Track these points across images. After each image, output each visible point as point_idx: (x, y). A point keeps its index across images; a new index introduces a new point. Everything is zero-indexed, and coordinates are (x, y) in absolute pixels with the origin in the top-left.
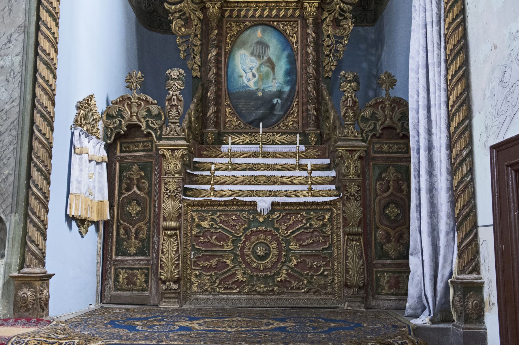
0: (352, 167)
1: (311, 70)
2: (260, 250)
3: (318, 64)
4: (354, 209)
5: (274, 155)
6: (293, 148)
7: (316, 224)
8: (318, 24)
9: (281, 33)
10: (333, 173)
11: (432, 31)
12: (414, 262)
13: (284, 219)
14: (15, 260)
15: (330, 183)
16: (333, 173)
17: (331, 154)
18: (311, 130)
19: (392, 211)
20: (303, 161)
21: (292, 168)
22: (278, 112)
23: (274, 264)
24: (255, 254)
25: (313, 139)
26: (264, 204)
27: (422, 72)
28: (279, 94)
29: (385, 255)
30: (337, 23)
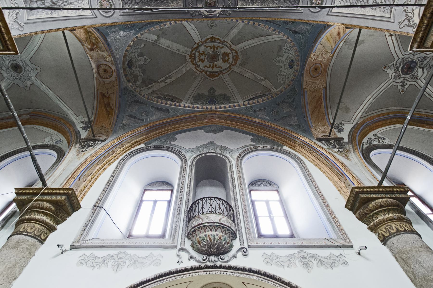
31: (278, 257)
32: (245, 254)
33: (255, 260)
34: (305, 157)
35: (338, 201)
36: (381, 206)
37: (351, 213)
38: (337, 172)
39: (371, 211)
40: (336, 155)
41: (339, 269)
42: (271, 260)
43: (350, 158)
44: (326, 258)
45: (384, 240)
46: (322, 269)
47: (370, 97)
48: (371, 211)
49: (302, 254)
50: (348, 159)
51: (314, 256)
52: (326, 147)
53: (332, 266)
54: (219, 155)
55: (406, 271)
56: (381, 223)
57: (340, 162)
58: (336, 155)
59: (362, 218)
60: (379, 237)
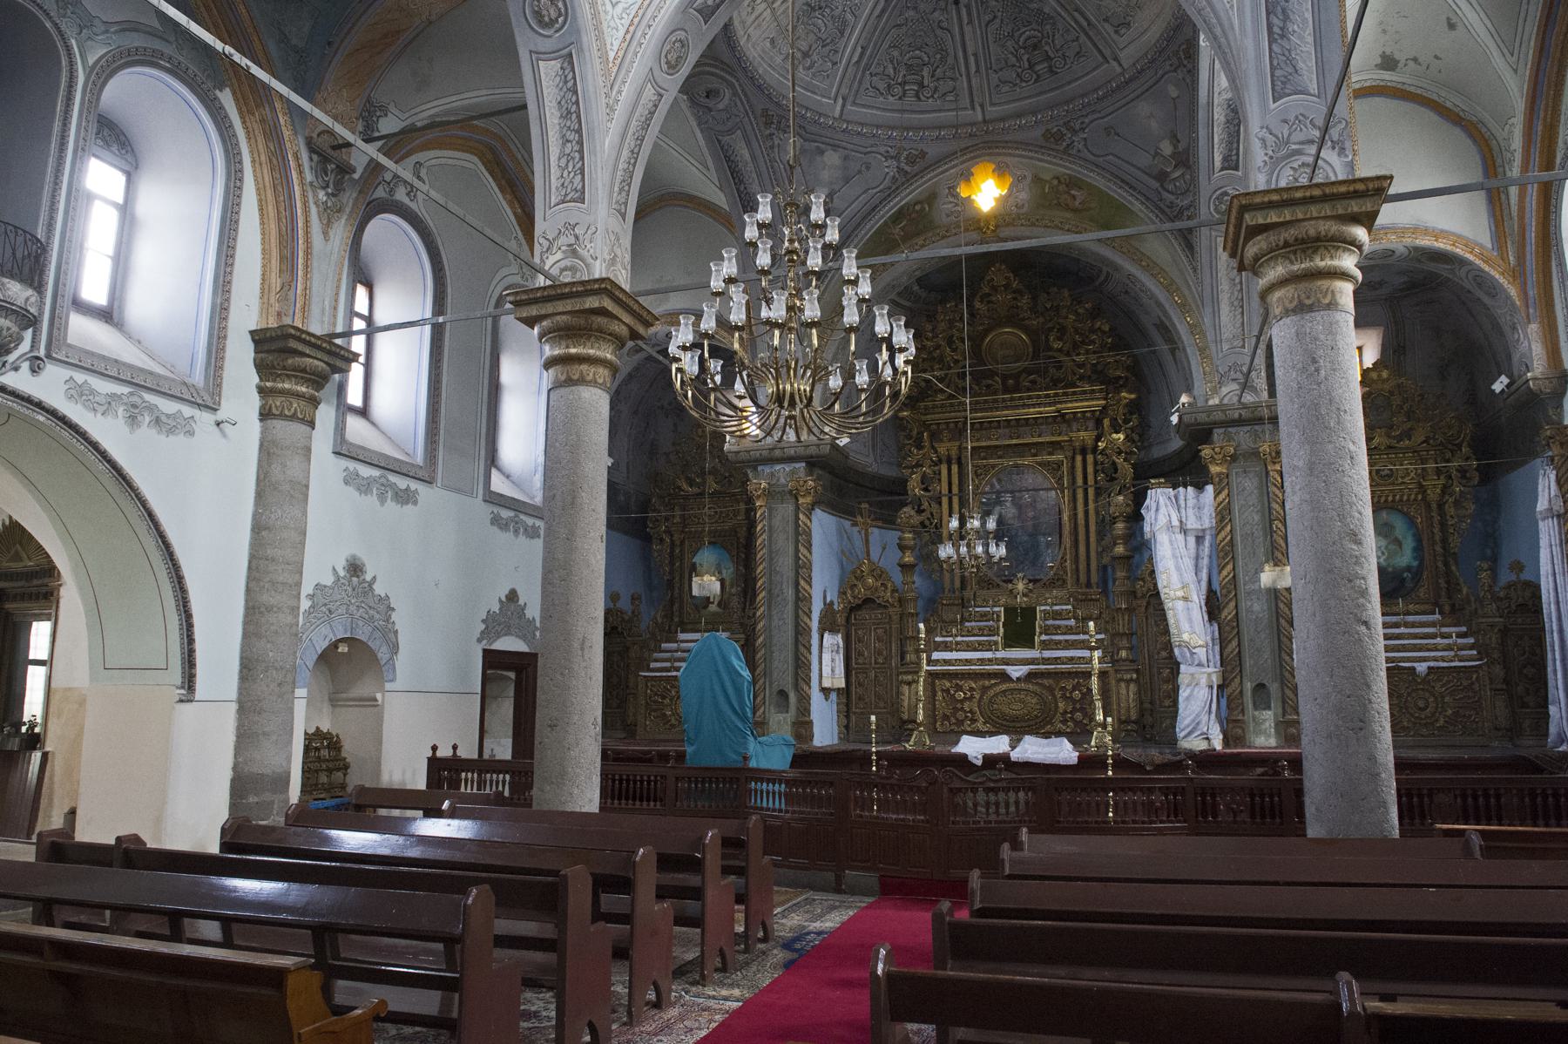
0: (1493, 639)
1: (1438, 549)
2: (1421, 704)
3: (1444, 541)
4: (1498, 670)
5: (1413, 625)
6: (1431, 618)
7: (1465, 683)
8: (1441, 506)
9: (1406, 515)
10: (1471, 640)
11: (1556, 550)
12: (1553, 710)
13: (1439, 680)
14: (1280, 711)
15: (1472, 647)
16: (1471, 640)
17: (1468, 623)
18: (1444, 600)
19: (1530, 671)
20: (1444, 630)
21: (1433, 636)
22: (1409, 585)
23: (1433, 714)
24: (1416, 705)
25: (1447, 608)
26: (1421, 668)
27: (1551, 579)
28: (1408, 569)
29: (1524, 705)
30: (1457, 503)
31: (93, 392)
32: (35, 370)
33: (50, 386)
34: (253, 161)
35: (247, 315)
36: (304, 371)
37: (250, 346)
38: (286, 253)
39: (284, 368)
40: (314, 210)
41: (179, 440)
42: (79, 393)
43: (331, 233)
44: (168, 416)
45: (265, 415)
46: (153, 432)
47: (484, 92)
48: (284, 368)
49: (135, 399)
50: (325, 234)
51: (151, 408)
52: (309, 177)
53: (171, 431)
54: (48, 25)
55: (260, 466)
56: (282, 392)
57: (308, 241)
58: (314, 210)
59: (260, 367)
60: (262, 408)
